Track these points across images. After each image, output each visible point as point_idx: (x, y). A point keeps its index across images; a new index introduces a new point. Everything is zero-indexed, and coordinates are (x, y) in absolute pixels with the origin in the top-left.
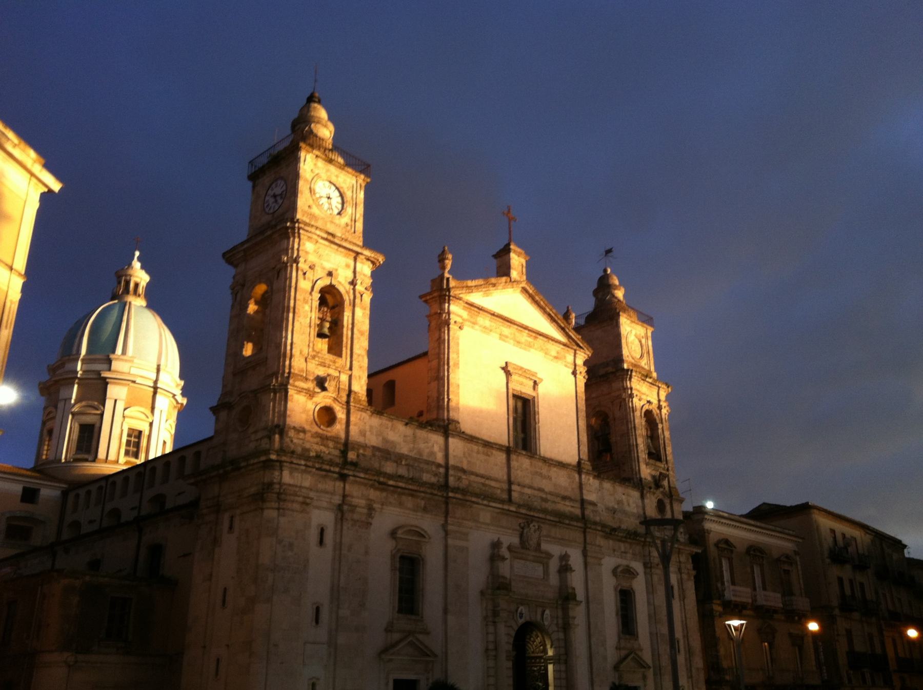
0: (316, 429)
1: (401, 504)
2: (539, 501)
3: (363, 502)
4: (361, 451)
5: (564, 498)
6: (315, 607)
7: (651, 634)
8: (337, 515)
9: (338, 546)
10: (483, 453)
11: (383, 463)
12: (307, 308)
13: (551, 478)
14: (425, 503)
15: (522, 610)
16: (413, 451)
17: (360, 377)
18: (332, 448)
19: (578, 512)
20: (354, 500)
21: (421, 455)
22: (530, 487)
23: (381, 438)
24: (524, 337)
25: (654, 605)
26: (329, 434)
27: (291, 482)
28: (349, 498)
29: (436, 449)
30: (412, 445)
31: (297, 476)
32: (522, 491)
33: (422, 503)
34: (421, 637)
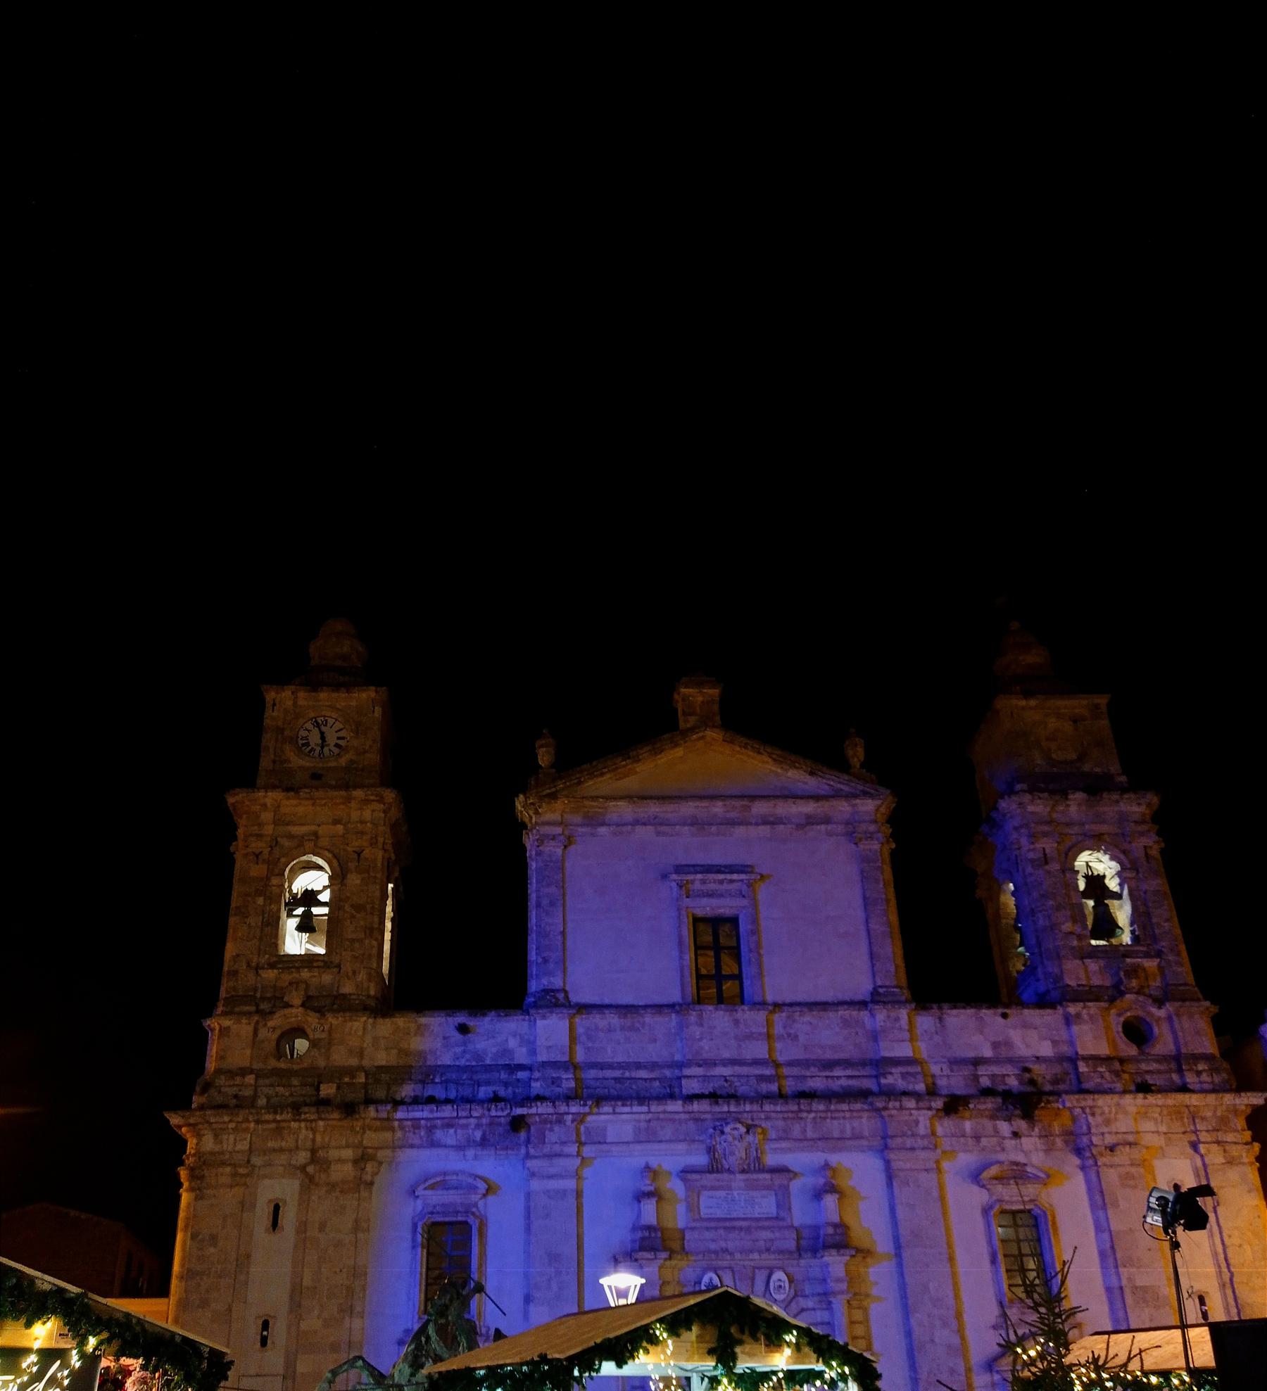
1: (433, 1144)
2: (753, 1081)
3: (348, 1153)
4: (347, 1080)
5: (829, 1065)
6: (260, 1322)
7: (1109, 1290)
9: (302, 1228)
10: (622, 1028)
13: (797, 1036)
15: (711, 1279)
17: (354, 972)
21: (478, 1056)
23: (395, 1052)
25: (1110, 1231)
27: (217, 1148)
29: (512, 1043)
31: (227, 1139)
32: (708, 1074)
33: (478, 1135)
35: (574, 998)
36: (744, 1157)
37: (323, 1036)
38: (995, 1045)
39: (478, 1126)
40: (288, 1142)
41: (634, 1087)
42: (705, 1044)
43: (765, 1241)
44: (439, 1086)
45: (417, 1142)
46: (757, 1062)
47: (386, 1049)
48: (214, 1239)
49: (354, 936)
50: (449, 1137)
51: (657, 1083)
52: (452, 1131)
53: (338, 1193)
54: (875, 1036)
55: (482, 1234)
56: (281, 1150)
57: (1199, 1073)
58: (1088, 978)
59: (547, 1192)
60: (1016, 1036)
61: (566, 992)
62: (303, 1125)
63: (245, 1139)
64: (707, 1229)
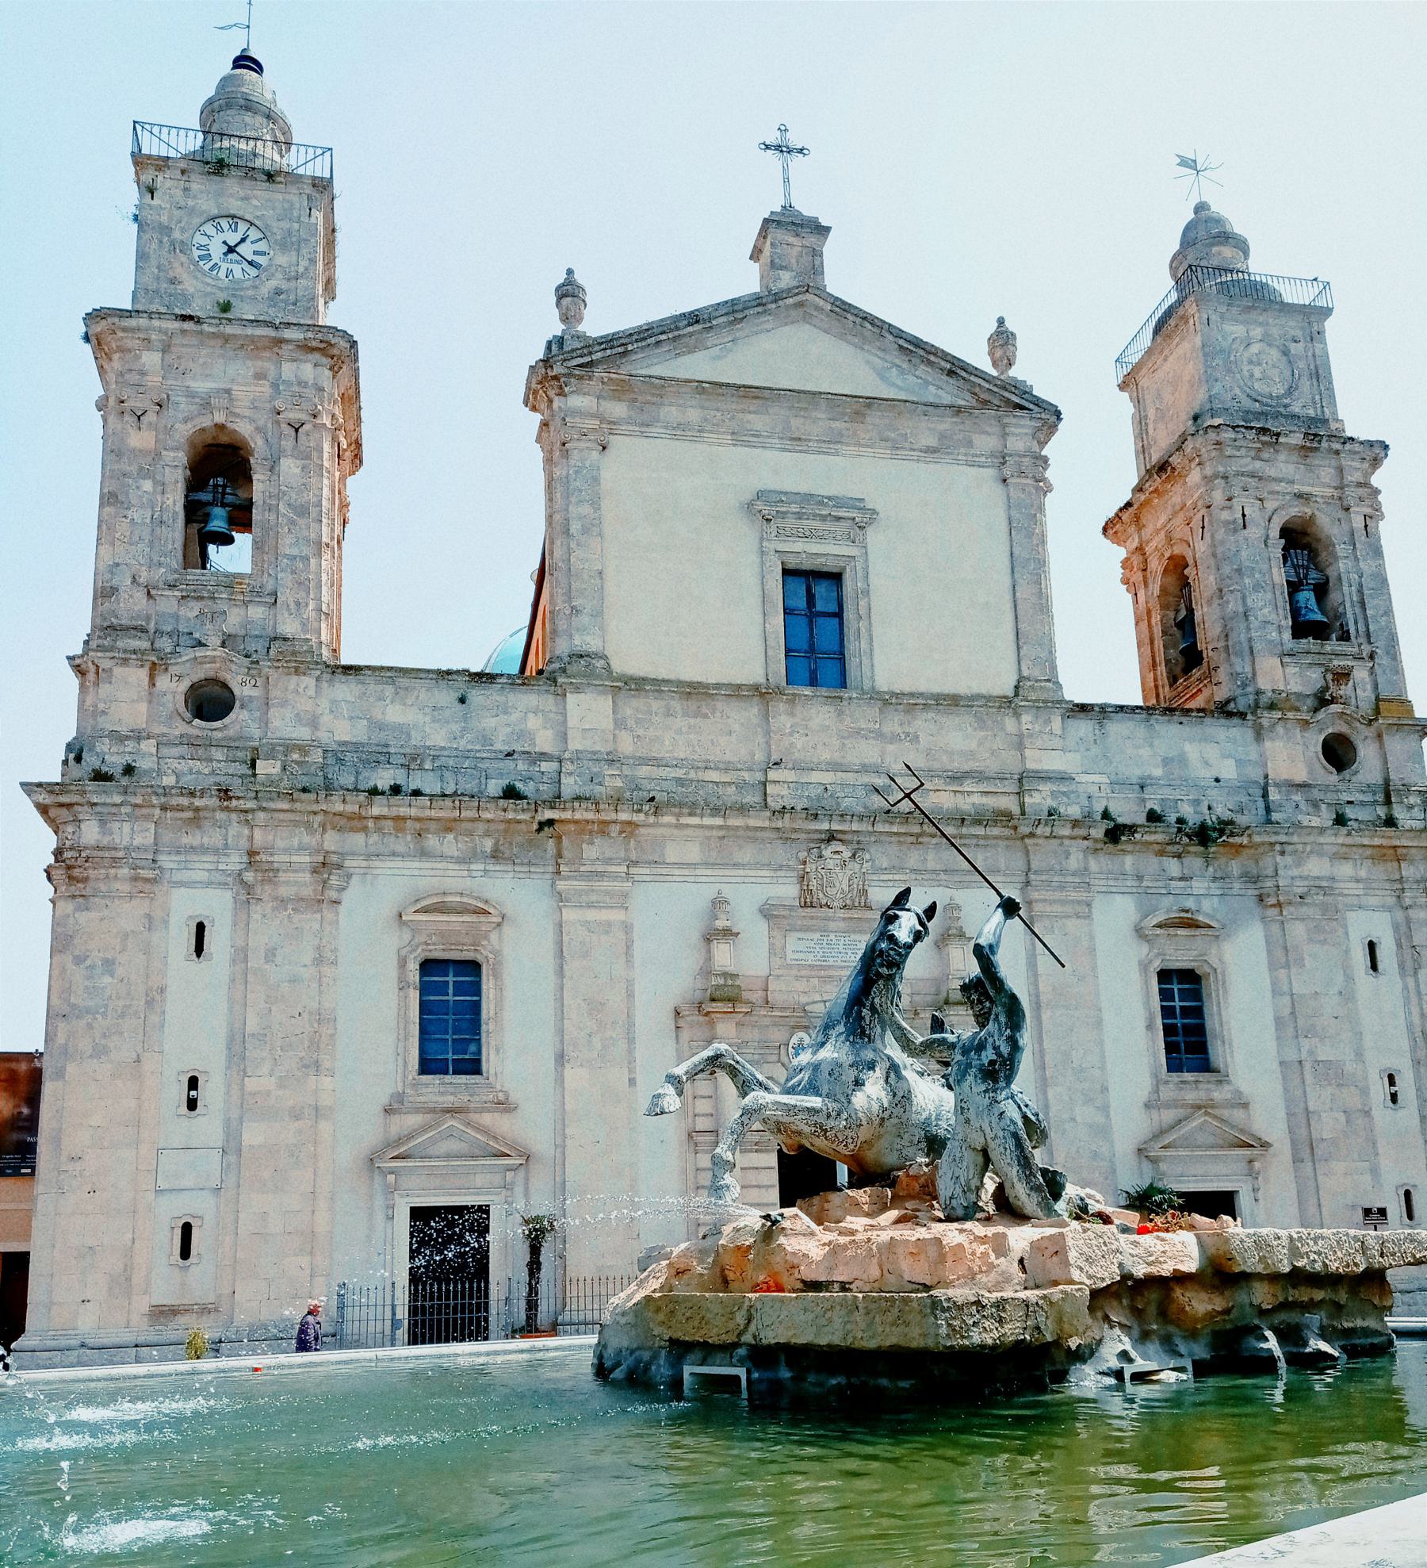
0: (180, 728)
1: (424, 854)
4: (296, 756)
5: (957, 777)
8: (237, 894)
9: (241, 955)
11: (365, 773)
12: (147, 485)
14: (496, 844)
16: (462, 737)
17: (298, 604)
18: (220, 761)
19: (1010, 804)
20: (276, 858)
21: (486, 740)
22: (835, 767)
24: (818, 423)
26: (218, 735)
27: (105, 841)
28: (263, 857)
29: (533, 722)
30: (455, 728)
33: (488, 844)
34: (487, 1119)
35: (618, 667)
36: (846, 889)
37: (255, 693)
38: (1166, 761)
39: (487, 834)
40: (212, 837)
41: (700, 792)
42: (799, 742)
44: (431, 774)
45: (400, 847)
46: (865, 769)
47: (351, 718)
48: (109, 965)
49: (295, 551)
50: (450, 844)
51: (732, 790)
52: (450, 837)
53: (290, 911)
54: (1020, 743)
55: (497, 975)
56: (203, 849)
57: (1411, 807)
58: (1287, 683)
59: (586, 924)
60: (1192, 751)
61: (604, 657)
62: (234, 816)
63: (147, 830)
64: (797, 978)
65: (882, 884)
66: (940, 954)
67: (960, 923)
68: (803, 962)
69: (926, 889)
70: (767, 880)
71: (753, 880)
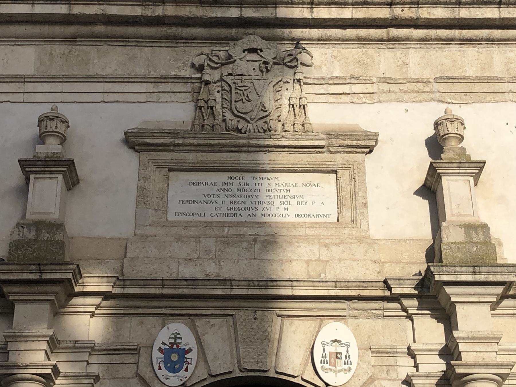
15: (176, 337)
43: (308, 262)
64: (179, 239)
65: (331, 99)
66: (460, 226)
67: (463, 144)
68: (197, 218)
69: (404, 106)
70: (143, 98)
71: (117, 97)
